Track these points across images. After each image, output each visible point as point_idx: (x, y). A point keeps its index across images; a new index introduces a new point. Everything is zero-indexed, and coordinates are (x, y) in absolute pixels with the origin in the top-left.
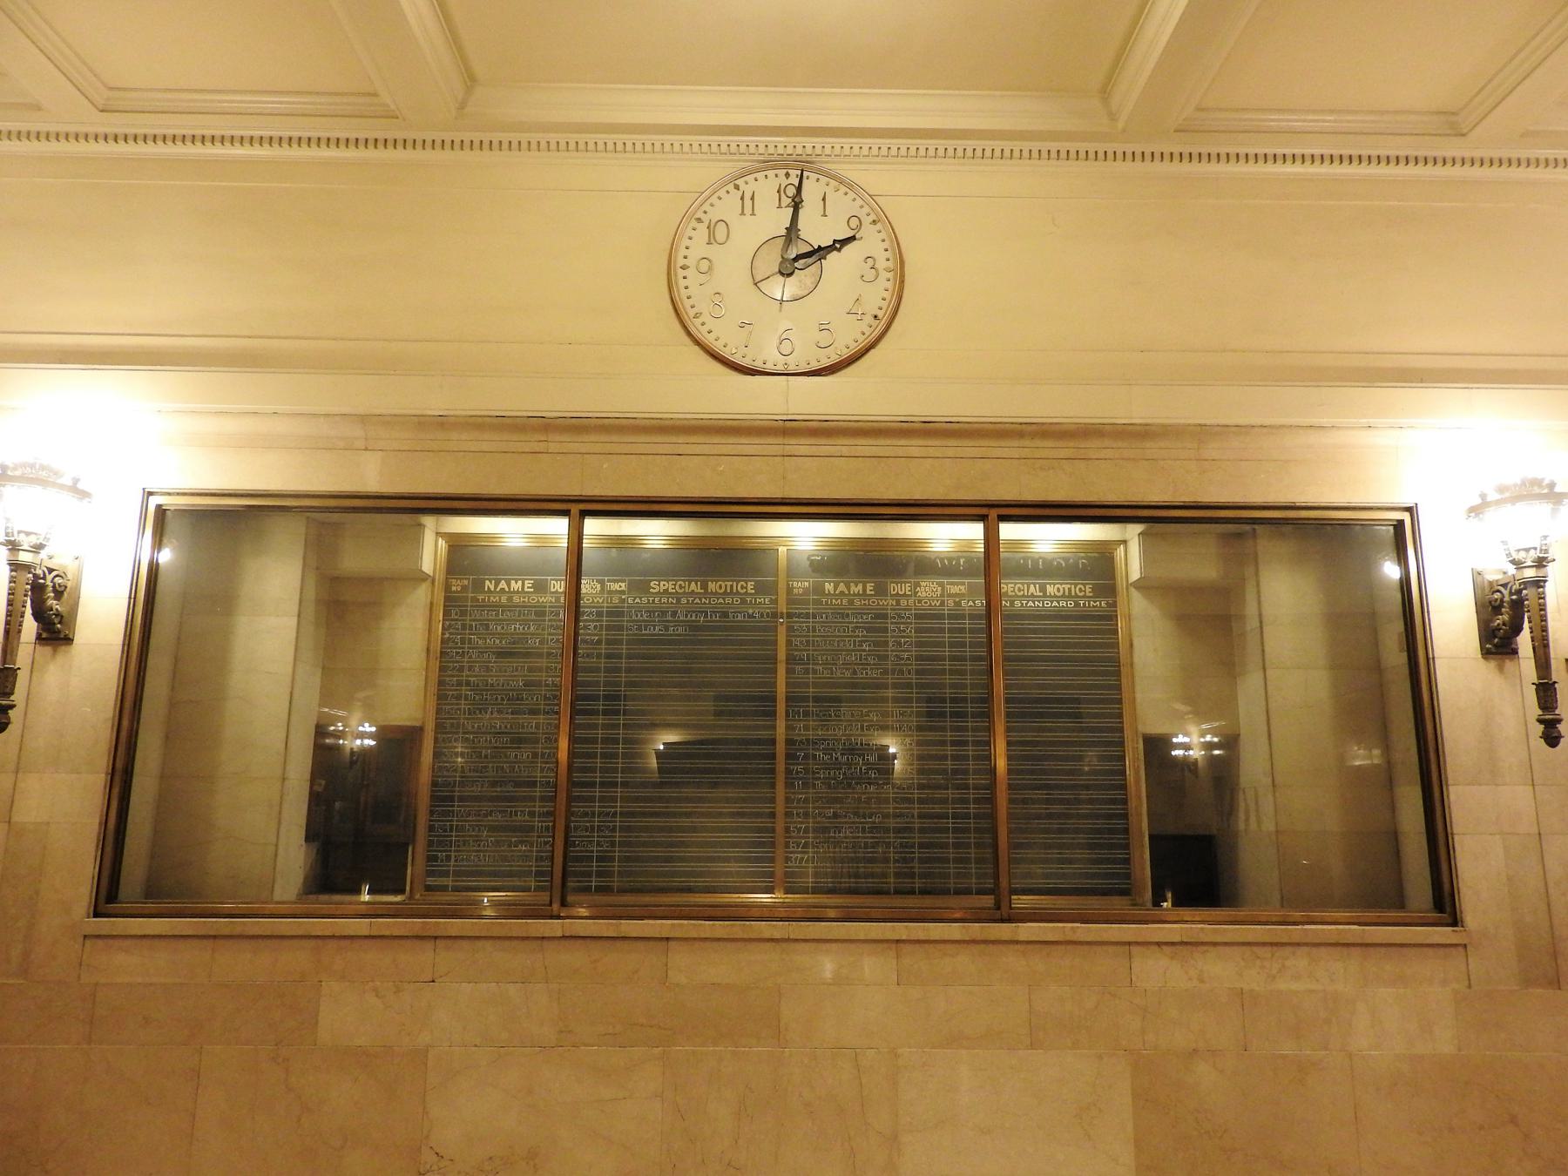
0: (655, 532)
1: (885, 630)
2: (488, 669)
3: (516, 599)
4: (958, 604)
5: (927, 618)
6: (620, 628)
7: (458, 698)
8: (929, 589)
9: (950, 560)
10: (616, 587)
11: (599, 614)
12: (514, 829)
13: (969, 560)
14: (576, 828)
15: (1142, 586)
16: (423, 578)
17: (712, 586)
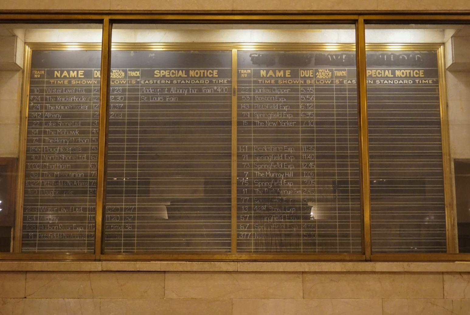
0: (157, 39)
1: (298, 98)
2: (57, 124)
3: (73, 82)
4: (342, 82)
5: (323, 90)
6: (137, 99)
7: (39, 141)
8: (323, 73)
9: (337, 56)
10: (133, 74)
11: (124, 90)
12: (72, 218)
13: (348, 56)
14: (110, 209)
15: (454, 69)
16: (16, 69)
17: (192, 73)
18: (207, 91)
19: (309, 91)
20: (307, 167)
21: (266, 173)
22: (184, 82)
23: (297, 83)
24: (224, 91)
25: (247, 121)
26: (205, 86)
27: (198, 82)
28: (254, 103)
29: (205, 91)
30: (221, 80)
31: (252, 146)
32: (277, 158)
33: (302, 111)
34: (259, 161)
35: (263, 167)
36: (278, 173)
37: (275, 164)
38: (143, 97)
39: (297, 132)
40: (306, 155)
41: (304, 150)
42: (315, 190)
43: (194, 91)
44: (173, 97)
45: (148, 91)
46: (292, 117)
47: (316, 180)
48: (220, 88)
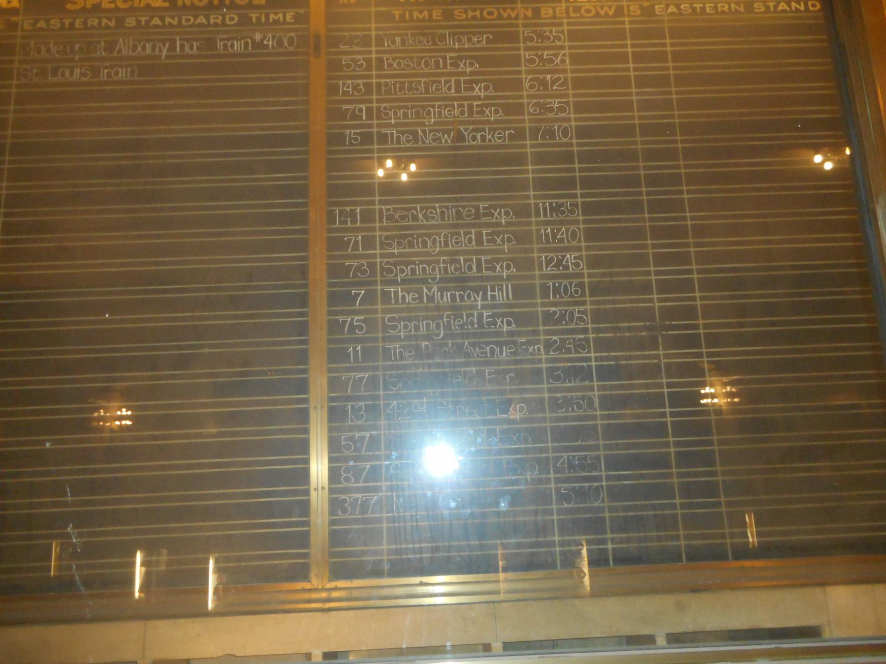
18: (232, 46)
19: (548, 38)
20: (557, 266)
21: (425, 290)
22: (160, 23)
23: (513, 15)
24: (286, 44)
25: (358, 131)
26: (227, 32)
27: (204, 21)
28: (379, 76)
29: (225, 46)
30: (276, 14)
31: (377, 207)
32: (457, 243)
33: (529, 97)
34: (400, 255)
35: (413, 271)
36: (464, 289)
37: (452, 261)
38: (26, 70)
39: (520, 160)
40: (552, 231)
41: (545, 215)
42: (587, 340)
43: (191, 48)
44: (122, 67)
45: (43, 49)
46: (501, 116)
47: (588, 307)
48: (273, 38)
